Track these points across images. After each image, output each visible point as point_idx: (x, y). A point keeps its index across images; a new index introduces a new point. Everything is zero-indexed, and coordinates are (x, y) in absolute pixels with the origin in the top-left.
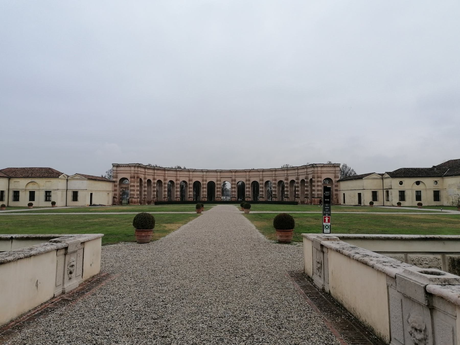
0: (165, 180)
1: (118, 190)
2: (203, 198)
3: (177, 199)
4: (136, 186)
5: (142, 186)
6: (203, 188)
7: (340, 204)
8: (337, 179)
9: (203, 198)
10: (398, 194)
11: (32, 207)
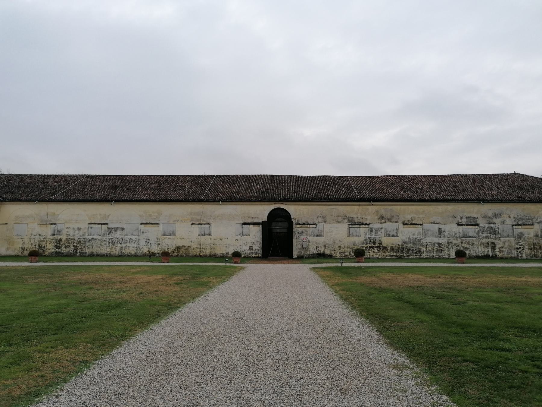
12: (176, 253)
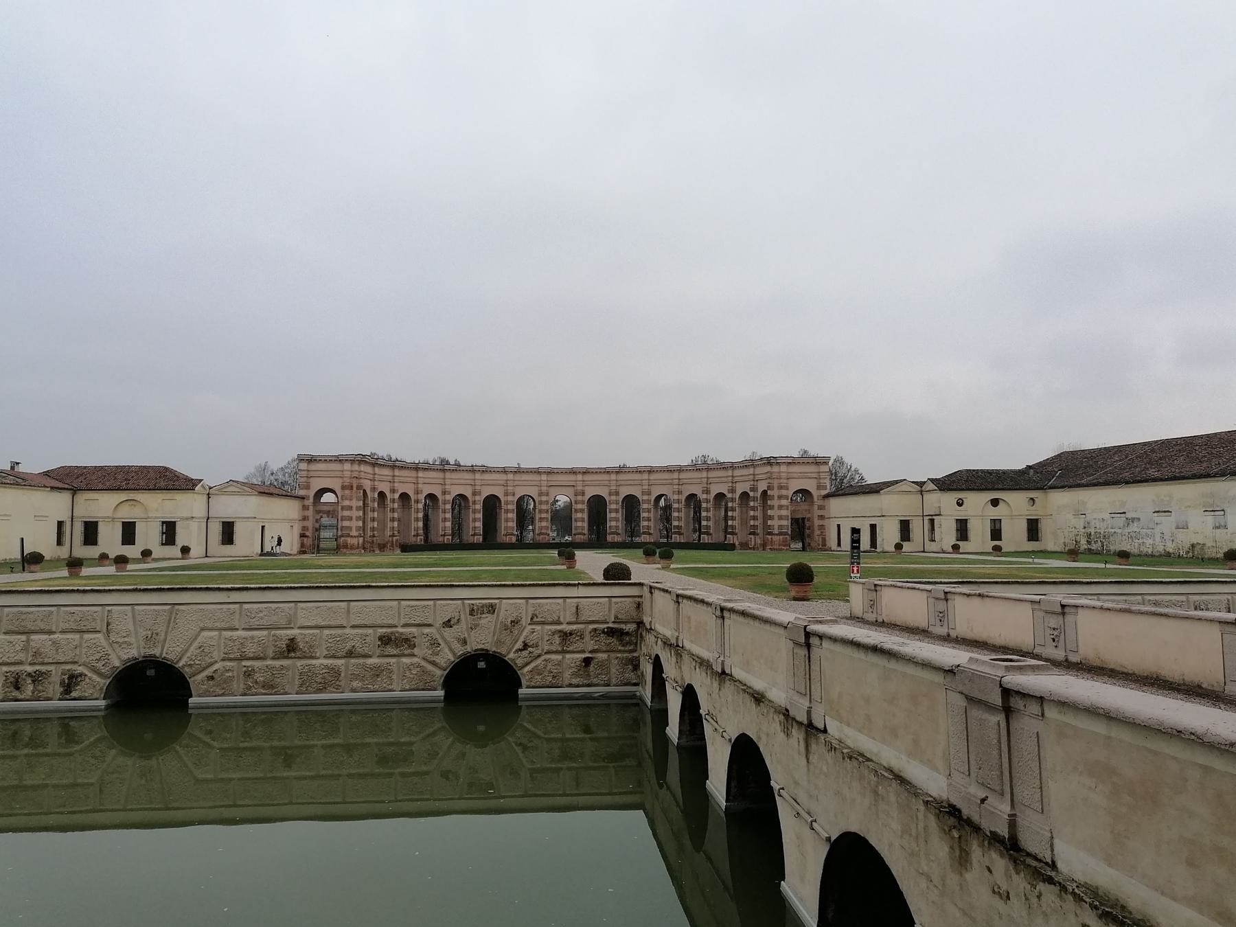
0: (417, 492)
1: (311, 518)
2: (506, 535)
3: (446, 537)
4: (354, 509)
5: (366, 508)
6: (507, 511)
7: (830, 548)
8: (824, 492)
9: (506, 535)
10: (953, 526)
11: (149, 559)
12: (1191, 554)
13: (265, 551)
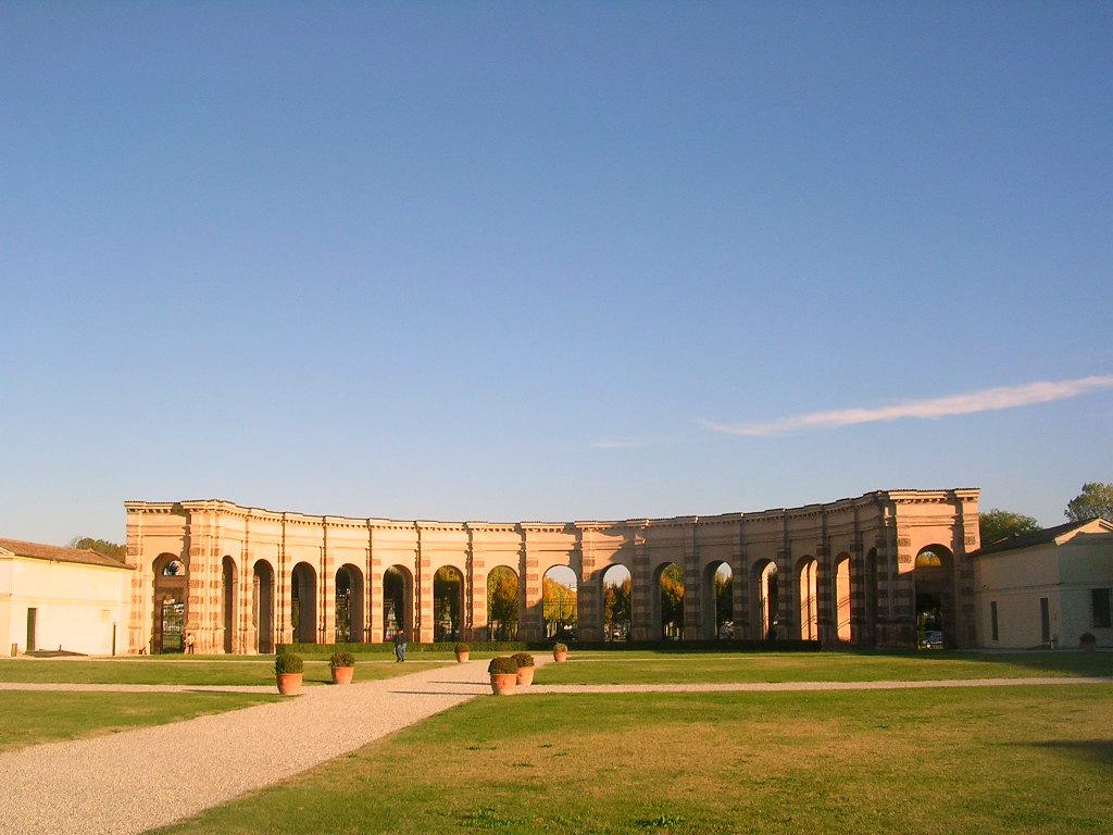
8: (969, 549)
13: (37, 649)
